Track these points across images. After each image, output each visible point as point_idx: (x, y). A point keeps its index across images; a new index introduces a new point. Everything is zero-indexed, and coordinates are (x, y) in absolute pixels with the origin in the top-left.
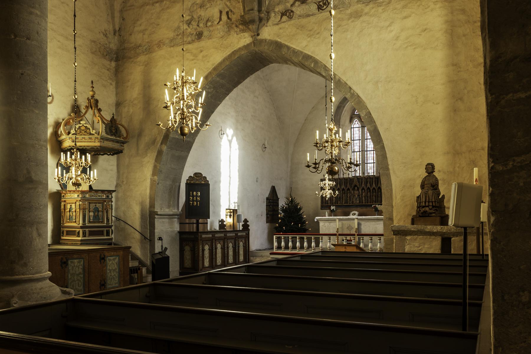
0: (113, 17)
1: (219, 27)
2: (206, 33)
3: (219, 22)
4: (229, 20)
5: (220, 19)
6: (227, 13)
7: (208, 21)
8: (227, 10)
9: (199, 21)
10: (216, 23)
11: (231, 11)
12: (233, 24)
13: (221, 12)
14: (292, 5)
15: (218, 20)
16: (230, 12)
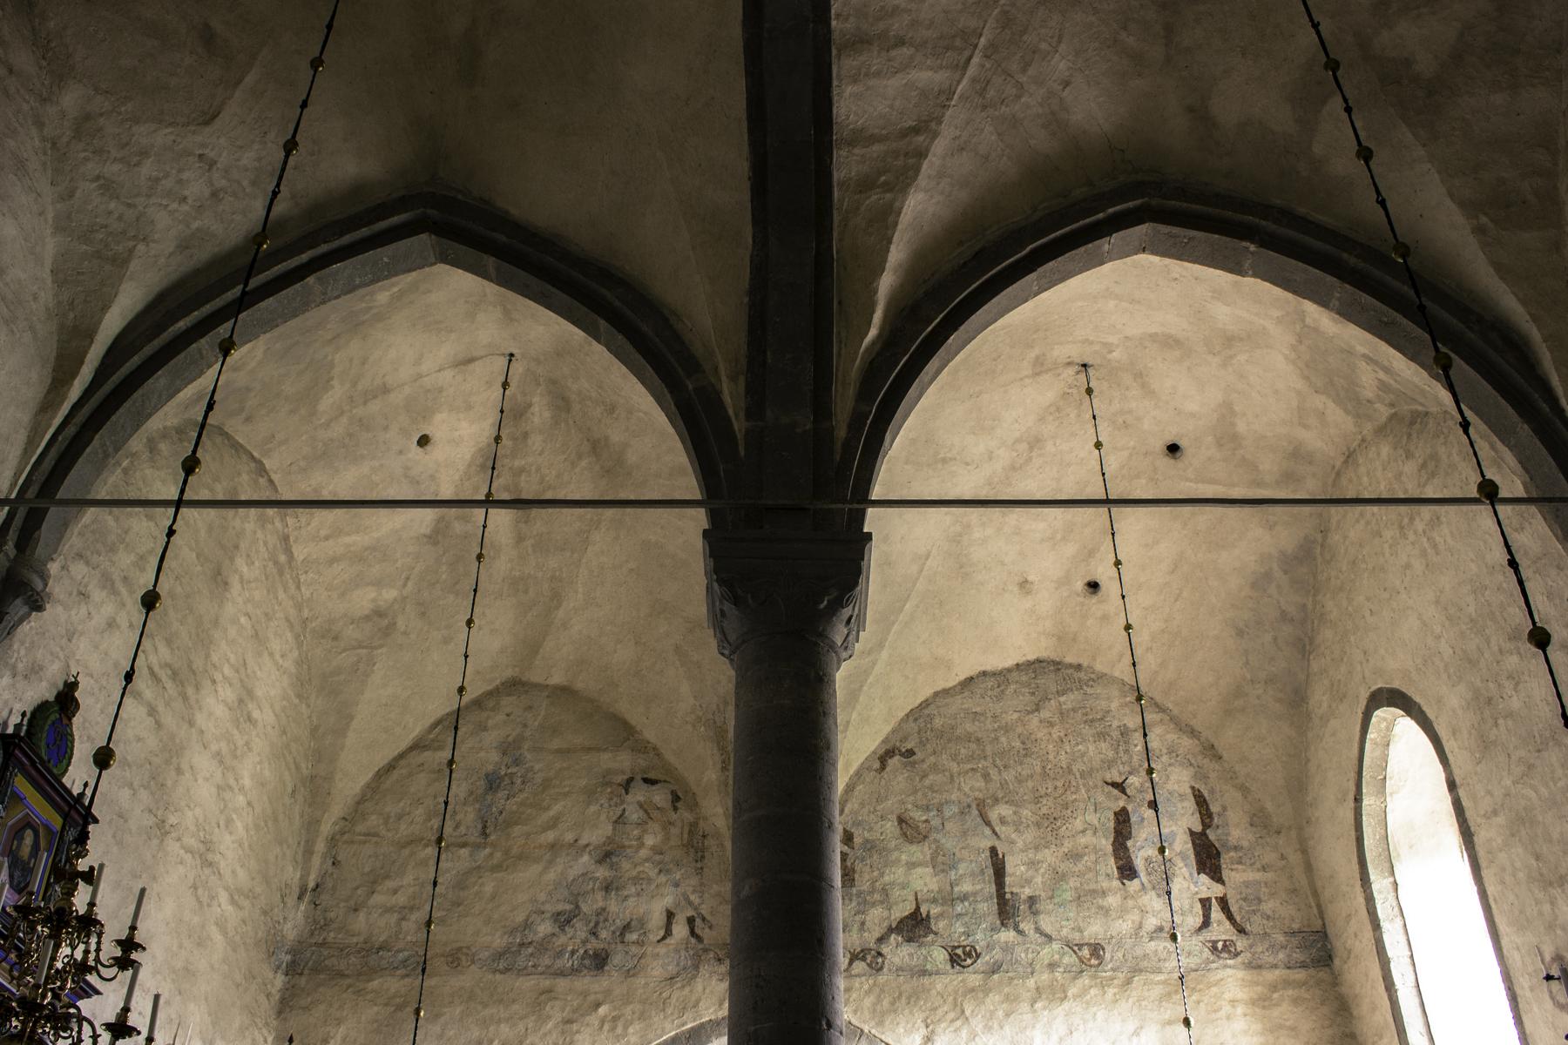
0: (309, 852)
1: (661, 949)
2: (616, 959)
3: (664, 938)
4: (693, 940)
5: (668, 932)
6: (691, 921)
7: (627, 928)
8: (690, 913)
9: (597, 924)
10: (654, 937)
11: (704, 919)
12: (706, 950)
13: (670, 915)
14: (881, 940)
15: (662, 933)
16: (698, 922)
